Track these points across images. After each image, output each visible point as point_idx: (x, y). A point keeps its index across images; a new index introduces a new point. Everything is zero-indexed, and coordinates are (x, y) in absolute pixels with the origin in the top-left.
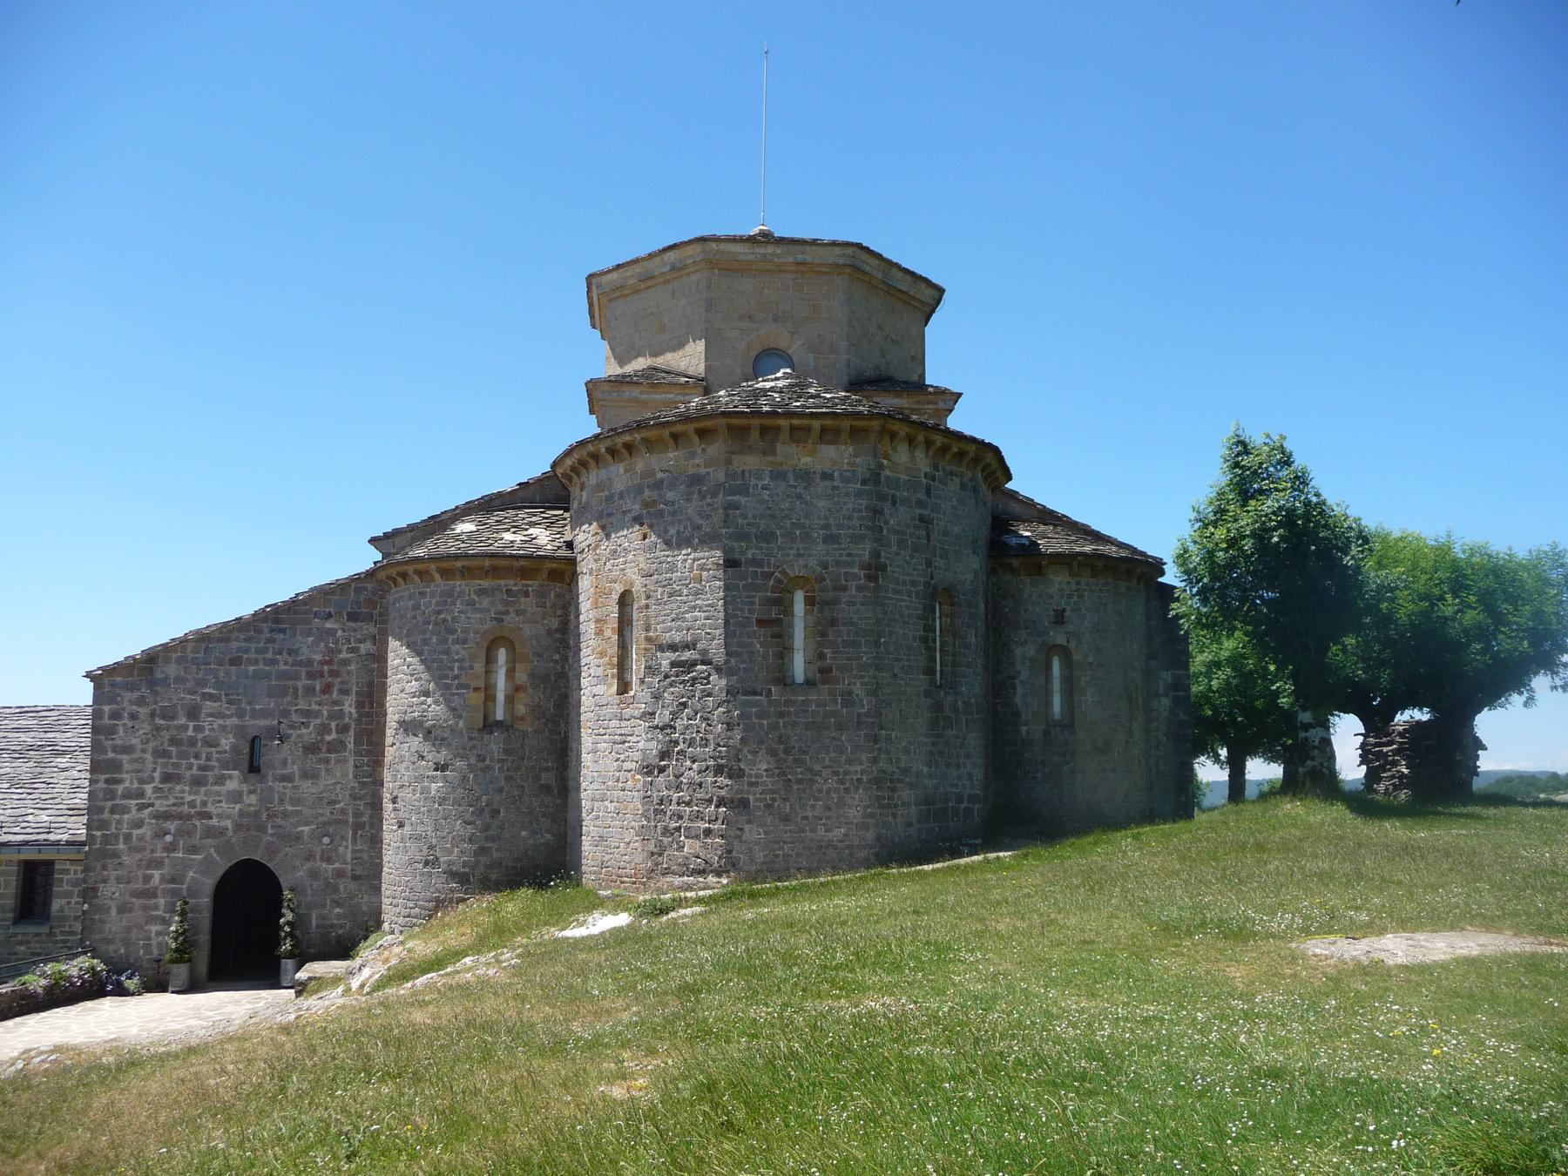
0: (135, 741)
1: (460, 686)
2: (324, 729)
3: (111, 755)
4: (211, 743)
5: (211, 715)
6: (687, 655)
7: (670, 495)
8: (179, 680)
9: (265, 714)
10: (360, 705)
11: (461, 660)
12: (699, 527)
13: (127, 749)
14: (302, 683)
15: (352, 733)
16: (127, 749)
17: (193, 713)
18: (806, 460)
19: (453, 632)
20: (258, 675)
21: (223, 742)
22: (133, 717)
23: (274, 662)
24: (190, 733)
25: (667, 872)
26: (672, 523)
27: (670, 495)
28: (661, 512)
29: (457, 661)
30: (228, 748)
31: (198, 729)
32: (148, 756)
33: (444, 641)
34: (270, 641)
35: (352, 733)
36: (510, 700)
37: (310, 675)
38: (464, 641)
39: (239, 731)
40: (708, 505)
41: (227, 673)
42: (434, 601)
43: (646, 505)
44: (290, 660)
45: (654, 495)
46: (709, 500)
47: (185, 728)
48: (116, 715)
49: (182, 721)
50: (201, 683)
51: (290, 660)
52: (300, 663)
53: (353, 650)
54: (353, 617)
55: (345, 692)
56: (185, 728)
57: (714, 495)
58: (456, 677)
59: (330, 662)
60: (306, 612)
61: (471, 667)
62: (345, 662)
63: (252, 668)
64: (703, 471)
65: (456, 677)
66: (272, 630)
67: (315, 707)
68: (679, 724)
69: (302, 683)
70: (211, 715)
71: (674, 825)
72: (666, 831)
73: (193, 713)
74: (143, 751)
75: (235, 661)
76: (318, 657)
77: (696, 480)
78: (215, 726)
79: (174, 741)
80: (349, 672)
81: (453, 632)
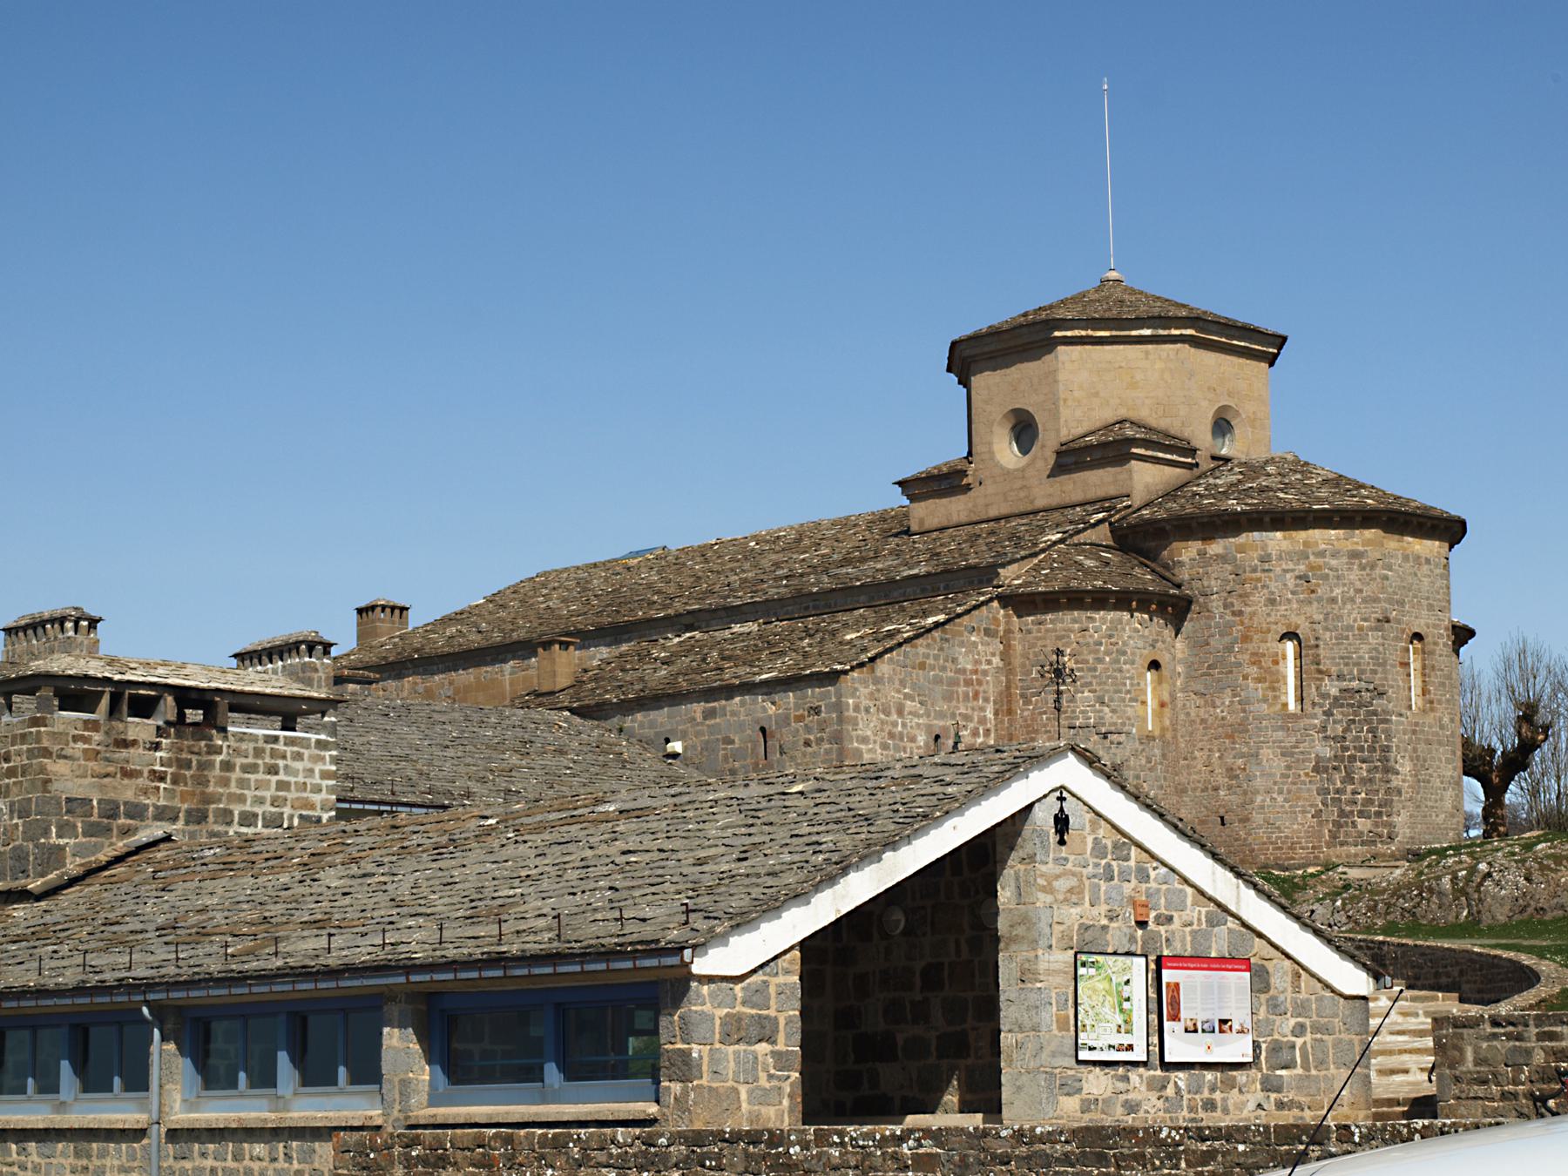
0: (869, 733)
1: (1131, 700)
2: (975, 734)
3: (856, 744)
4: (913, 739)
5: (910, 713)
6: (1355, 684)
7: (1334, 562)
8: (891, 680)
9: (941, 715)
10: (996, 714)
11: (1131, 678)
12: (1361, 591)
13: (865, 740)
14: (962, 689)
15: (992, 735)
16: (865, 740)
17: (900, 712)
18: (1417, 547)
19: (1124, 653)
20: (938, 681)
21: (919, 738)
22: (867, 710)
23: (943, 669)
24: (900, 728)
25: (1342, 844)
26: (1337, 585)
27: (1334, 562)
28: (1328, 575)
29: (1128, 678)
30: (922, 744)
31: (904, 725)
32: (879, 751)
33: (1118, 661)
34: (941, 649)
35: (992, 735)
36: (1158, 715)
37: (968, 683)
38: (1133, 663)
39: (929, 727)
40: (1368, 575)
41: (917, 675)
42: (1104, 627)
43: (1312, 568)
44: (953, 667)
45: (1320, 561)
46: (1368, 570)
47: (895, 724)
48: (857, 708)
49: (894, 717)
50: (903, 683)
51: (953, 667)
52: (958, 671)
53: (989, 662)
54: (987, 632)
55: (986, 700)
56: (895, 724)
57: (1373, 567)
58: (1128, 692)
59: (976, 672)
60: (960, 625)
61: (1139, 684)
62: (985, 673)
63: (932, 673)
64: (1360, 548)
65: (1128, 692)
66: (942, 639)
67: (969, 712)
68: (1348, 735)
69: (962, 689)
70: (910, 713)
71: (1348, 808)
72: (1342, 813)
73: (900, 712)
74: (875, 742)
75: (922, 666)
76: (969, 667)
77: (1355, 555)
78: (914, 724)
79: (891, 735)
80: (988, 682)
81: (1124, 653)
